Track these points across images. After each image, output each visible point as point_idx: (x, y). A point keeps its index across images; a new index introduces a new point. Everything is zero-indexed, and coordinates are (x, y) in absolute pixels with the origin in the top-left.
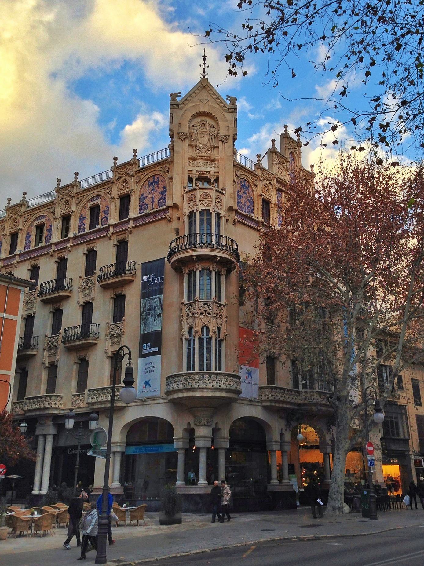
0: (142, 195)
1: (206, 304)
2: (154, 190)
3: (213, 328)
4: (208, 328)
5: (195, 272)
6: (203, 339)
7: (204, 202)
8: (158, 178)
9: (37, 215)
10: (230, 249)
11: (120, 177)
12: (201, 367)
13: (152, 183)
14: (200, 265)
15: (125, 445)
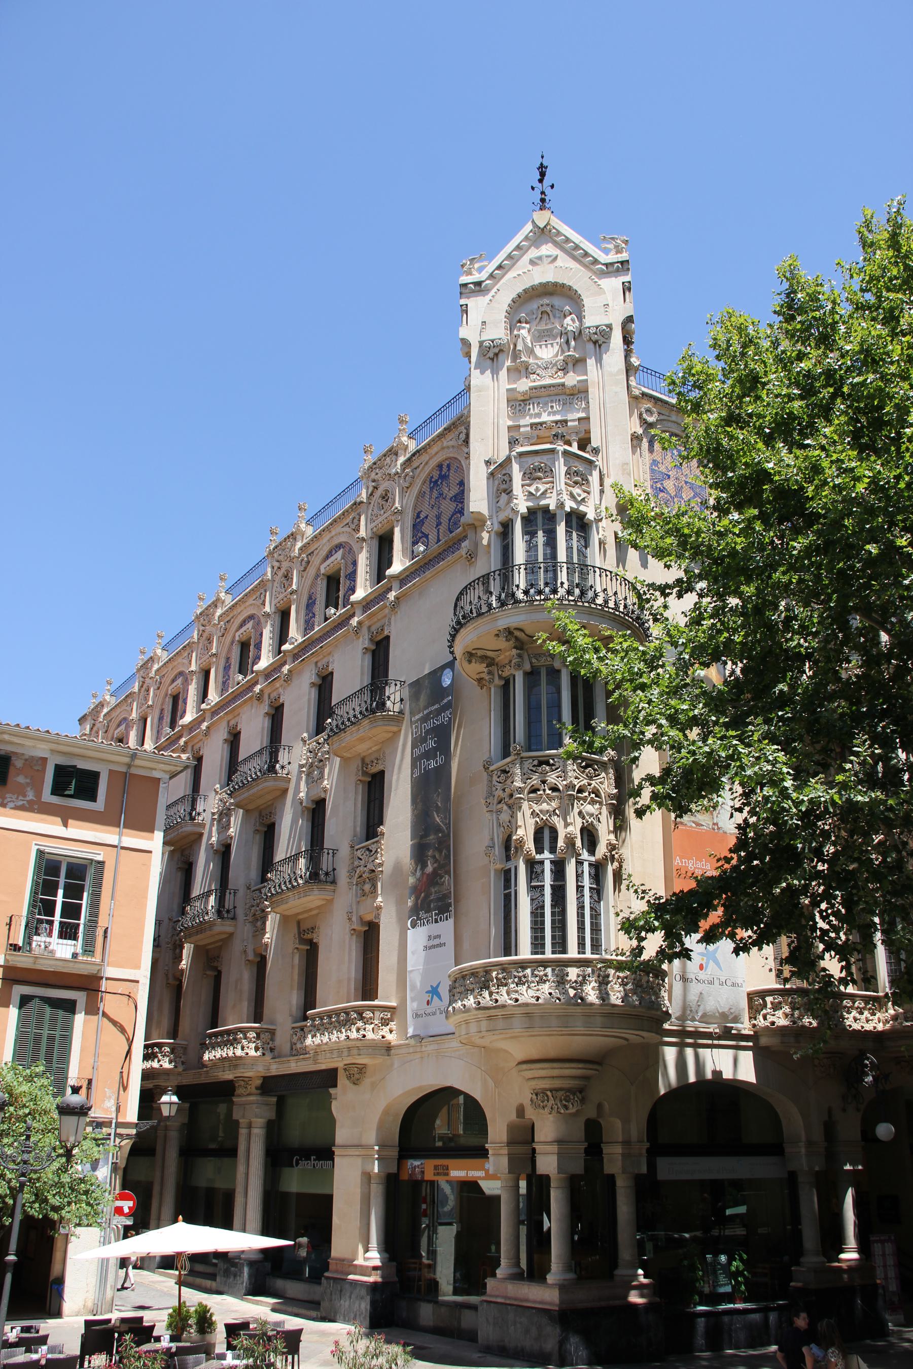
0: (418, 517)
1: (548, 763)
2: (441, 494)
3: (569, 828)
4: (554, 832)
5: (514, 676)
6: (542, 863)
7: (532, 489)
8: (449, 466)
9: (241, 618)
10: (625, 606)
11: (376, 488)
12: (538, 945)
13: (436, 481)
14: (526, 657)
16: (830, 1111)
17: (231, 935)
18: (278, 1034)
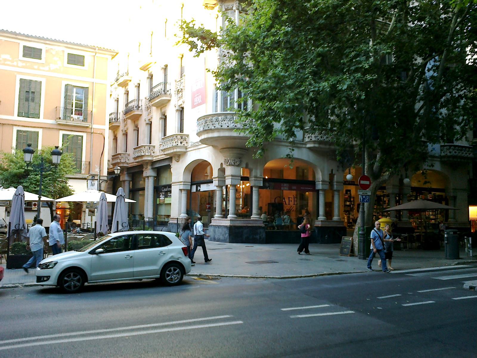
14: (223, 6)
15: (190, 184)
16: (332, 170)
17: (141, 115)
18: (156, 147)
